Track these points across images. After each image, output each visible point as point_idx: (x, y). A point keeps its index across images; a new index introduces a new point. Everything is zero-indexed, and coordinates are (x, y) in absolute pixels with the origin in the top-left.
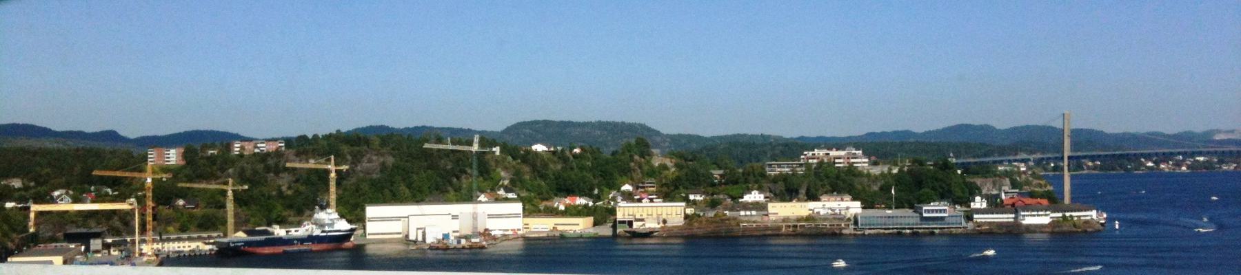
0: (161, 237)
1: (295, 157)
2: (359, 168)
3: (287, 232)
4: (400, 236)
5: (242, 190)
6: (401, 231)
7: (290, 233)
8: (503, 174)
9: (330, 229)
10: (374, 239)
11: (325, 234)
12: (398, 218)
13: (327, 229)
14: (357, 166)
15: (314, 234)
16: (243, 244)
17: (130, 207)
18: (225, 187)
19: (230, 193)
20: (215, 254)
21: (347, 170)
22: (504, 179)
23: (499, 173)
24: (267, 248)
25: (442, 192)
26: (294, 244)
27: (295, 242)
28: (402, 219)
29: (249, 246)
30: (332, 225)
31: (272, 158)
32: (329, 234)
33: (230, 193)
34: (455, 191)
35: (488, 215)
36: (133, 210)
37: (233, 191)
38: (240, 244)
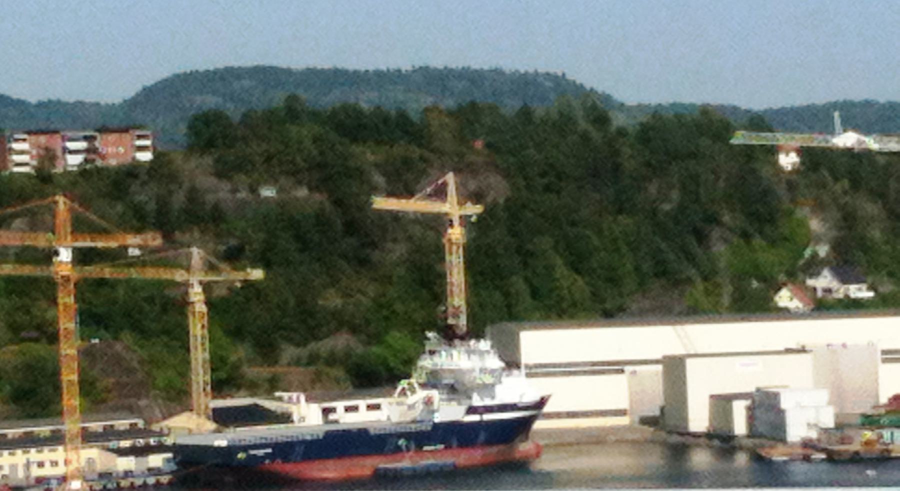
1: (213, 180)
3: (326, 412)
4: (624, 421)
5: (245, 281)
6: (624, 405)
7: (332, 417)
8: (815, 225)
9: (488, 402)
10: (576, 431)
11: (475, 418)
12: (616, 367)
13: (477, 401)
15: (438, 418)
16: (269, 450)
19: (196, 294)
20: (170, 483)
21: (480, 216)
22: (818, 240)
23: (803, 224)
24: (330, 463)
25: (677, 283)
26: (398, 449)
27: (402, 442)
28: (628, 369)
29: (286, 459)
30: (487, 388)
31: (144, 184)
32: (488, 417)
33: (196, 294)
34: (705, 279)
35: (884, 352)
37: (207, 287)
38: (261, 452)
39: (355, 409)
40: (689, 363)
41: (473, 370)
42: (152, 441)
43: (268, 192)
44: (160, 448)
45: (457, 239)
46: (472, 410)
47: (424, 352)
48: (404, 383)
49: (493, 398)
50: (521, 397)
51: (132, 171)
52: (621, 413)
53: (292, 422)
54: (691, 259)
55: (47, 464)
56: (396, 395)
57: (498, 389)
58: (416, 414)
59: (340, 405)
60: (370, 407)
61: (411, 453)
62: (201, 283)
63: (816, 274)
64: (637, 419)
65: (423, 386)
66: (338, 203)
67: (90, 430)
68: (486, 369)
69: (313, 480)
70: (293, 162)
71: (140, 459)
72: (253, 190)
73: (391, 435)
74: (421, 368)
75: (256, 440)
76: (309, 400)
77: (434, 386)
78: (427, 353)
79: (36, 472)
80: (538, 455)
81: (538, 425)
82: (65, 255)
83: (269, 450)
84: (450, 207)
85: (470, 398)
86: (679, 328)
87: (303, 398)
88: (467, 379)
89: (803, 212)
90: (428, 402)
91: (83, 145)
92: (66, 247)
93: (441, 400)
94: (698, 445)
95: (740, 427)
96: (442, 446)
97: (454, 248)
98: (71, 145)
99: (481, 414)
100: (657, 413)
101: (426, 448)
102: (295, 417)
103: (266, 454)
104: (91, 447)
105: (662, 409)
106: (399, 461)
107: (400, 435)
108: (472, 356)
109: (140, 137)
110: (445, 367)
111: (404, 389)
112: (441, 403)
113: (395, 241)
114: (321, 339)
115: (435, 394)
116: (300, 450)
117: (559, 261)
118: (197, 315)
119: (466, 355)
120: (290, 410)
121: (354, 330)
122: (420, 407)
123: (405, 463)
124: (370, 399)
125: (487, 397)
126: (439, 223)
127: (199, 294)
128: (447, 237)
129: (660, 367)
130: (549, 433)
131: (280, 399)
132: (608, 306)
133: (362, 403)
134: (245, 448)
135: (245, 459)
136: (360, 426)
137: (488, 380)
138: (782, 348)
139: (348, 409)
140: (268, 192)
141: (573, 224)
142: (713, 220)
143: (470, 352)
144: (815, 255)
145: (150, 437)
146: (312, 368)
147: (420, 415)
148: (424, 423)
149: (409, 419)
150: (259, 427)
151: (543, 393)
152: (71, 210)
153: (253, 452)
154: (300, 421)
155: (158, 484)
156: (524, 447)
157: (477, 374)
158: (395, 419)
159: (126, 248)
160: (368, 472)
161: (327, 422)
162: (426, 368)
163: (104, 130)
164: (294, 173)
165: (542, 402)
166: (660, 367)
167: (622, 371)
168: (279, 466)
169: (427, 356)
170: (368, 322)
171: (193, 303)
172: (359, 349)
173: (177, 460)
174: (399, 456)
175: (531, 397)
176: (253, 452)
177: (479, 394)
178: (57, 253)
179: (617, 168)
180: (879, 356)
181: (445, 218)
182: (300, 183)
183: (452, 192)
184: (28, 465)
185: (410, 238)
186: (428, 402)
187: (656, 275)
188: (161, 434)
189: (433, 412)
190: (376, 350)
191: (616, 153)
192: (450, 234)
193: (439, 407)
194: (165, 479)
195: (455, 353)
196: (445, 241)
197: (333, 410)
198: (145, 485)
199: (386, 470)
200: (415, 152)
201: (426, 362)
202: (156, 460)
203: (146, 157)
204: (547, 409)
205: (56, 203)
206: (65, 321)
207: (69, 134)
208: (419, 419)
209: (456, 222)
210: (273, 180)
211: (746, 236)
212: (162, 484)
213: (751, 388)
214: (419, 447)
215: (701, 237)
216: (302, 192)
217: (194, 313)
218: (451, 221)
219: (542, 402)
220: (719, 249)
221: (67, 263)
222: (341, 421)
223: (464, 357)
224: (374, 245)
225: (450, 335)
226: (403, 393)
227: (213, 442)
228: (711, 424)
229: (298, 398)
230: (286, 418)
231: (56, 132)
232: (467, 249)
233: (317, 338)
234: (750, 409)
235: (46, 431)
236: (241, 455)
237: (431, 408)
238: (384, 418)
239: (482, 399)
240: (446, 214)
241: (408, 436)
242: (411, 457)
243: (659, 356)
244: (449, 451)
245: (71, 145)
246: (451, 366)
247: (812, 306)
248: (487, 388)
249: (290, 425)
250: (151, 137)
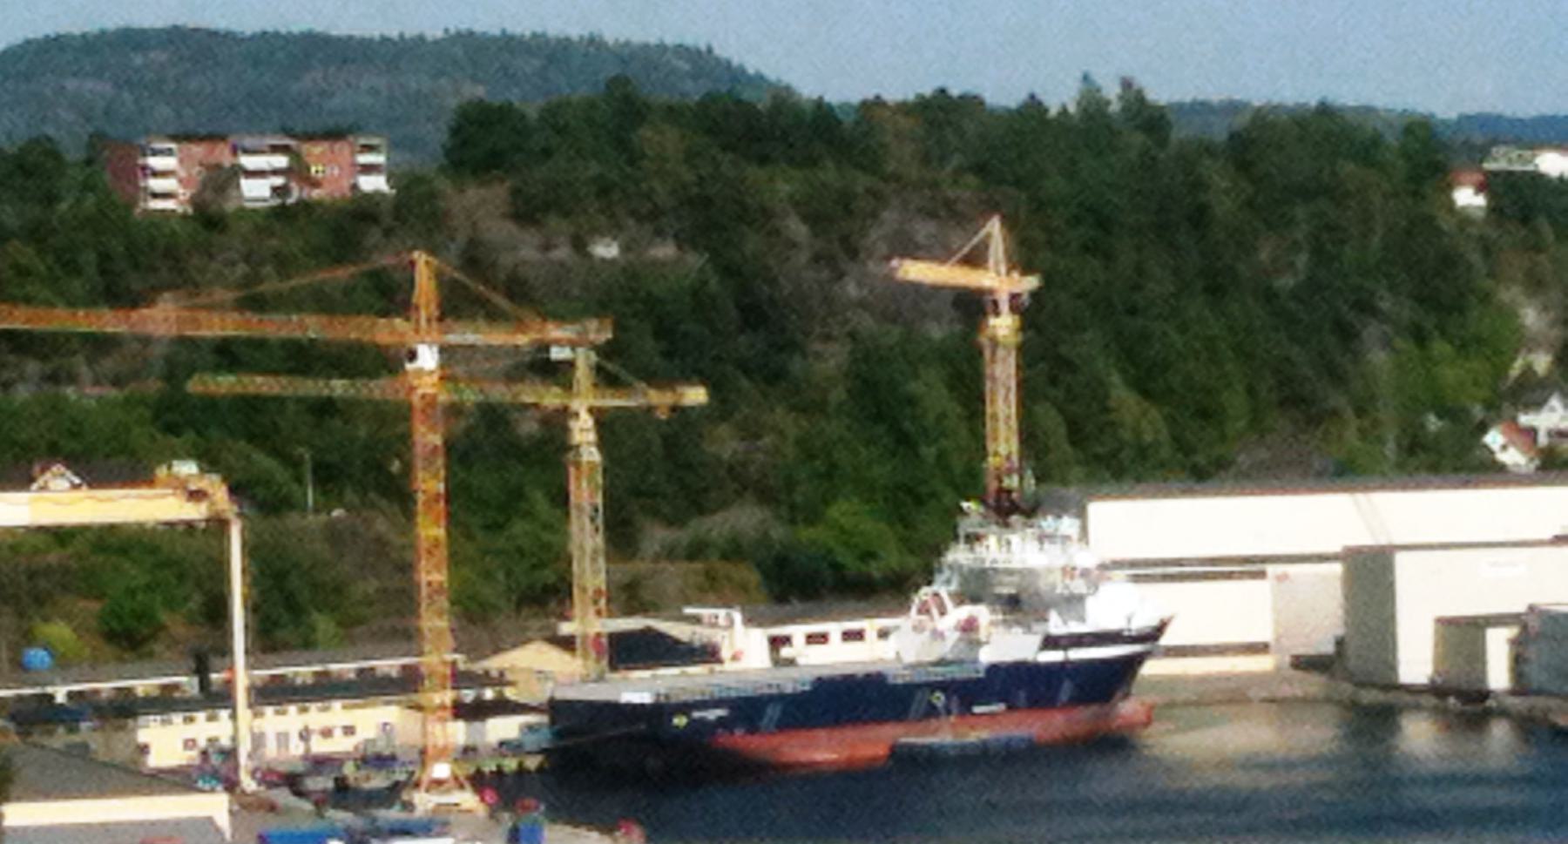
0: (204, 685)
1: (510, 227)
2: (852, 289)
3: (776, 643)
5: (674, 409)
6: (1263, 634)
7: (785, 652)
8: (1531, 317)
9: (1075, 628)
12: (1250, 567)
13: (1057, 625)
14: (840, 276)
15: (987, 656)
16: (720, 712)
17: (195, 512)
18: (551, 398)
19: (583, 431)
20: (540, 769)
21: (1034, 295)
22: (1532, 344)
23: (1509, 314)
26: (932, 712)
27: (939, 699)
28: (1271, 569)
29: (753, 729)
30: (1073, 603)
31: (388, 233)
33: (583, 431)
34: (1360, 412)
36: (218, 525)
37: (605, 422)
38: (712, 714)
39: (822, 638)
40: (1402, 561)
41: (1050, 571)
42: (489, 694)
43: (606, 250)
44: (503, 707)
45: (1004, 336)
46: (1050, 642)
47: (956, 538)
48: (925, 593)
49: (1082, 619)
50: (1129, 620)
51: (363, 211)
52: (1259, 648)
53: (720, 661)
54: (1337, 378)
55: (338, 733)
56: (914, 610)
57: (1091, 604)
58: (945, 649)
59: (798, 632)
61: (952, 719)
62: (591, 410)
63: (1538, 405)
64: (1287, 659)
65: (961, 598)
66: (728, 271)
68: (1074, 569)
69: (788, 766)
70: (648, 196)
71: (477, 725)
72: (580, 245)
73: (919, 686)
74: (951, 567)
75: (721, 691)
76: (750, 621)
77: (975, 600)
78: (962, 540)
79: (320, 746)
80: (1147, 723)
81: (1150, 668)
82: (428, 358)
83: (720, 712)
85: (1046, 620)
86: (1361, 497)
87: (737, 616)
88: (1043, 585)
89: (1509, 294)
90: (969, 626)
91: (281, 161)
92: (430, 345)
93: (993, 623)
94: (1418, 707)
95: (1498, 676)
96: (1000, 707)
97: (1001, 353)
98: (249, 162)
99: (1065, 648)
100: (1328, 648)
101: (977, 709)
102: (725, 653)
103: (720, 718)
104: (388, 703)
105: (1340, 643)
106: (935, 732)
107: (933, 686)
108: (1047, 545)
109: (369, 148)
110: (1000, 565)
111: (924, 603)
112: (993, 630)
113: (828, 338)
114: (713, 512)
115: (982, 613)
116: (773, 712)
117: (1116, 379)
118: (585, 468)
119: (1036, 544)
120: (714, 640)
121: (765, 496)
122: (953, 637)
123: (944, 735)
124: (850, 620)
125: (1073, 618)
126: (974, 305)
127: (588, 430)
128: (989, 332)
129: (1337, 568)
131: (697, 620)
132: (1200, 459)
133: (834, 629)
134: (685, 708)
135: (685, 727)
136: (872, 669)
137: (1079, 586)
138: (1547, 535)
139: (812, 639)
140: (606, 250)
141: (1132, 311)
142: (1366, 307)
143: (1042, 538)
144: (1528, 370)
145: (484, 686)
146: (698, 566)
147: (952, 650)
148: (965, 666)
149: (933, 657)
150: (662, 671)
151: (1164, 614)
152: (439, 276)
153: (696, 714)
154: (735, 658)
155: (521, 771)
156: (1128, 708)
157: (1057, 577)
158: (910, 657)
159: (545, 347)
160: (882, 751)
161: (778, 662)
162: (961, 567)
163: (310, 137)
164: (652, 217)
165: (1159, 630)
166: (1337, 568)
167: (1261, 575)
168: (740, 739)
169: (962, 546)
170: (790, 484)
171: (578, 447)
172: (778, 532)
173: (557, 727)
174: (934, 722)
175: (1143, 621)
176: (696, 714)
177: (1060, 614)
178: (413, 356)
179: (1199, 217)
181: (989, 298)
182: (659, 233)
183: (997, 253)
184: (305, 735)
185: (852, 335)
186: (969, 626)
187: (1282, 404)
188: (500, 681)
189: (979, 644)
191: (1199, 185)
192: (994, 327)
193: (989, 635)
194: (532, 763)
195: (1015, 539)
196: (983, 340)
197: (786, 640)
198: (499, 772)
199: (911, 747)
200: (862, 182)
201: (958, 555)
202: (503, 728)
203: (373, 183)
204: (1166, 640)
205: (412, 264)
206: (427, 476)
207: (248, 142)
208: (950, 657)
209: (1004, 307)
210: (613, 229)
211: (1420, 337)
212: (529, 772)
213: (1519, 607)
214: (966, 709)
215: (1347, 334)
216: (665, 251)
217: (578, 465)
218: (995, 303)
219: (1159, 630)
220: (1379, 357)
221: (432, 372)
222: (801, 661)
223: (1033, 546)
224: (791, 347)
225: (1006, 509)
226: (924, 610)
227: (619, 694)
228: (1437, 672)
230: (707, 654)
231: (222, 138)
232: (1022, 349)
233: (702, 511)
235: (349, 670)
236: (680, 721)
237: (973, 636)
238: (891, 655)
239: (1065, 622)
240: (991, 291)
241: (945, 686)
242: (953, 725)
243: (1335, 547)
244: (1016, 716)
245: (249, 162)
246: (1010, 562)
247: (1537, 462)
248: (1073, 603)
249: (717, 667)
250: (384, 149)
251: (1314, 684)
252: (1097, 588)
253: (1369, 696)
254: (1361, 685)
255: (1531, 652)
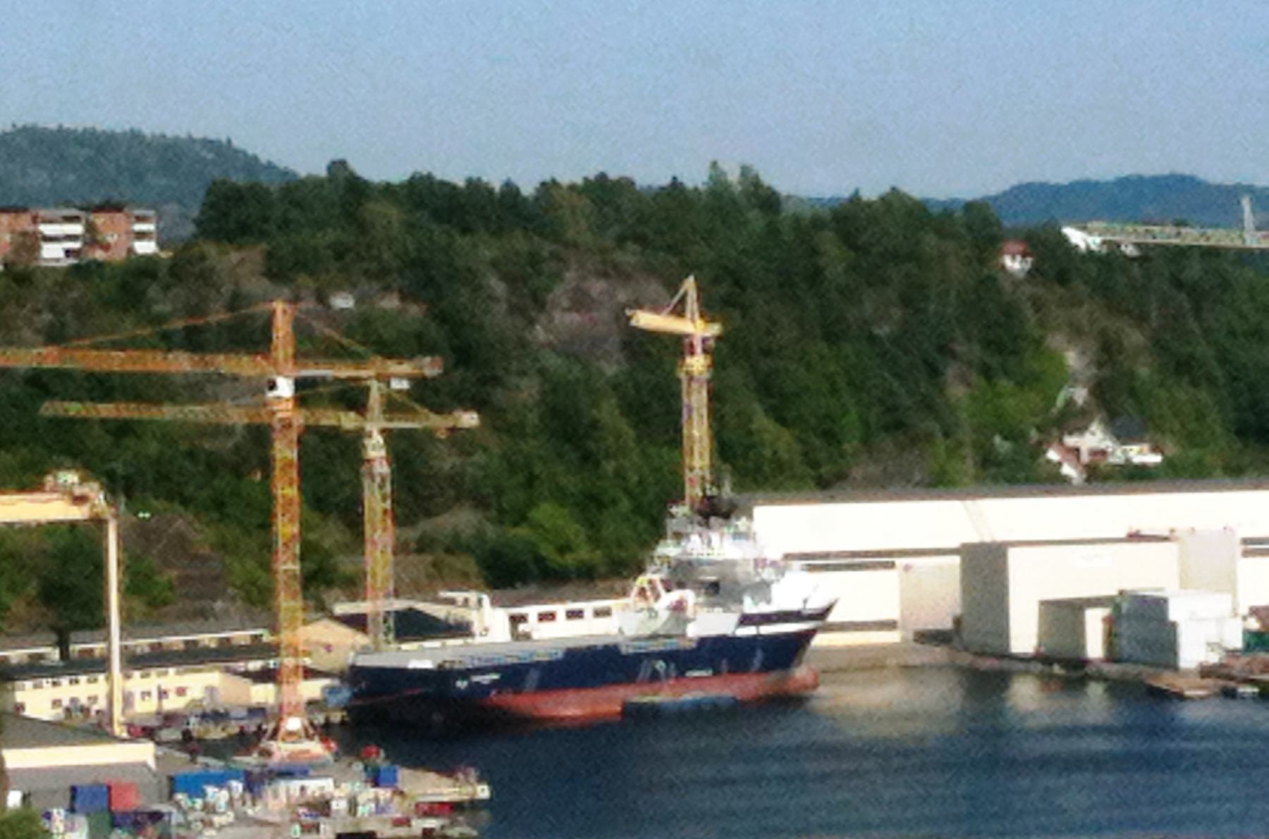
0: (64, 655)
1: (265, 283)
2: (540, 333)
3: (516, 620)
4: (892, 637)
5: (453, 430)
6: (893, 614)
7: (522, 627)
8: (1072, 358)
9: (764, 608)
10: (850, 650)
11: (750, 631)
12: (879, 560)
13: (750, 606)
14: (531, 322)
15: (694, 631)
16: (495, 677)
17: (77, 513)
18: (349, 421)
19: (375, 448)
20: (343, 723)
21: (719, 339)
22: (1075, 382)
24: (571, 696)
25: (914, 441)
26: (655, 677)
27: (660, 665)
28: (900, 562)
30: (762, 589)
31: (167, 288)
32: (766, 630)
33: (375, 448)
34: (947, 435)
35: (1246, 541)
36: (98, 523)
38: (486, 679)
39: (549, 617)
40: (1013, 553)
43: (343, 302)
46: (746, 620)
48: (642, 580)
49: (769, 602)
50: (805, 601)
51: (144, 269)
52: (890, 625)
54: (928, 406)
57: (776, 590)
58: (657, 625)
59: (532, 611)
60: (599, 613)
62: (383, 431)
63: (1081, 430)
64: (911, 636)
66: (442, 318)
67: (234, 642)
68: (765, 560)
70: (378, 259)
72: (322, 298)
74: (659, 557)
76: (494, 603)
77: (681, 585)
80: (815, 686)
81: (820, 641)
82: (285, 388)
84: (696, 328)
85: (741, 602)
86: (969, 503)
87: (486, 599)
88: (740, 572)
89: (1056, 340)
90: (678, 607)
91: (77, 229)
92: (286, 377)
94: (1027, 672)
95: (1095, 647)
97: (695, 386)
98: (47, 229)
100: (948, 625)
102: (476, 628)
105: (958, 621)
106: (655, 694)
109: (140, 219)
110: (705, 557)
112: (698, 609)
113: (523, 374)
114: (437, 515)
115: (689, 595)
116: (534, 676)
117: (757, 408)
121: (480, 503)
122: (664, 615)
123: (663, 696)
126: (678, 345)
129: (956, 560)
130: (827, 651)
131: (452, 602)
132: (825, 470)
133: (560, 609)
134: (466, 674)
135: (466, 688)
137: (767, 574)
138: (1123, 535)
139: (543, 617)
140: (343, 302)
141: (766, 353)
142: (945, 350)
144: (1070, 402)
146: (429, 558)
153: (476, 679)
156: (801, 673)
158: (630, 631)
161: (516, 636)
163: (100, 209)
164: (381, 274)
165: (827, 611)
166: (956, 560)
167: (891, 566)
168: (509, 699)
170: (499, 491)
171: (369, 461)
172: (491, 531)
174: (657, 685)
176: (476, 679)
178: (273, 386)
179: (815, 276)
180: (1240, 548)
181: (687, 341)
182: (387, 289)
185: (542, 372)
186: (678, 607)
187: (886, 429)
190: (523, 531)
191: (814, 252)
194: (336, 717)
195: (715, 537)
197: (524, 618)
200: (547, 248)
201: (668, 549)
203: (146, 248)
204: (832, 618)
207: (43, 213)
208: (662, 632)
209: (699, 349)
210: (350, 285)
211: (987, 373)
212: (334, 724)
213: (1111, 590)
214: (681, 674)
215: (934, 372)
216: (391, 303)
218: (692, 345)
219: (827, 611)
220: (957, 392)
222: (535, 636)
223: (728, 541)
224: (496, 381)
228: (1040, 645)
229: (480, 601)
230: (461, 629)
231: (24, 210)
233: (429, 514)
234: (1112, 625)
236: (462, 684)
238: (615, 631)
239: (756, 604)
240: (688, 336)
242: (672, 687)
243: (955, 544)
245: (47, 229)
247: (1084, 476)
249: (469, 640)
250: (154, 220)
251: (939, 654)
252: (783, 574)
253: (986, 664)
254: (981, 654)
255: (1124, 628)
